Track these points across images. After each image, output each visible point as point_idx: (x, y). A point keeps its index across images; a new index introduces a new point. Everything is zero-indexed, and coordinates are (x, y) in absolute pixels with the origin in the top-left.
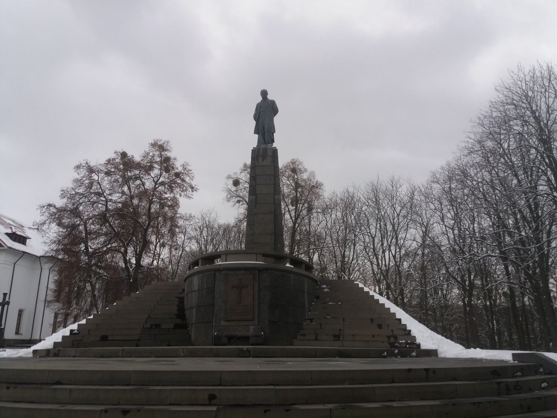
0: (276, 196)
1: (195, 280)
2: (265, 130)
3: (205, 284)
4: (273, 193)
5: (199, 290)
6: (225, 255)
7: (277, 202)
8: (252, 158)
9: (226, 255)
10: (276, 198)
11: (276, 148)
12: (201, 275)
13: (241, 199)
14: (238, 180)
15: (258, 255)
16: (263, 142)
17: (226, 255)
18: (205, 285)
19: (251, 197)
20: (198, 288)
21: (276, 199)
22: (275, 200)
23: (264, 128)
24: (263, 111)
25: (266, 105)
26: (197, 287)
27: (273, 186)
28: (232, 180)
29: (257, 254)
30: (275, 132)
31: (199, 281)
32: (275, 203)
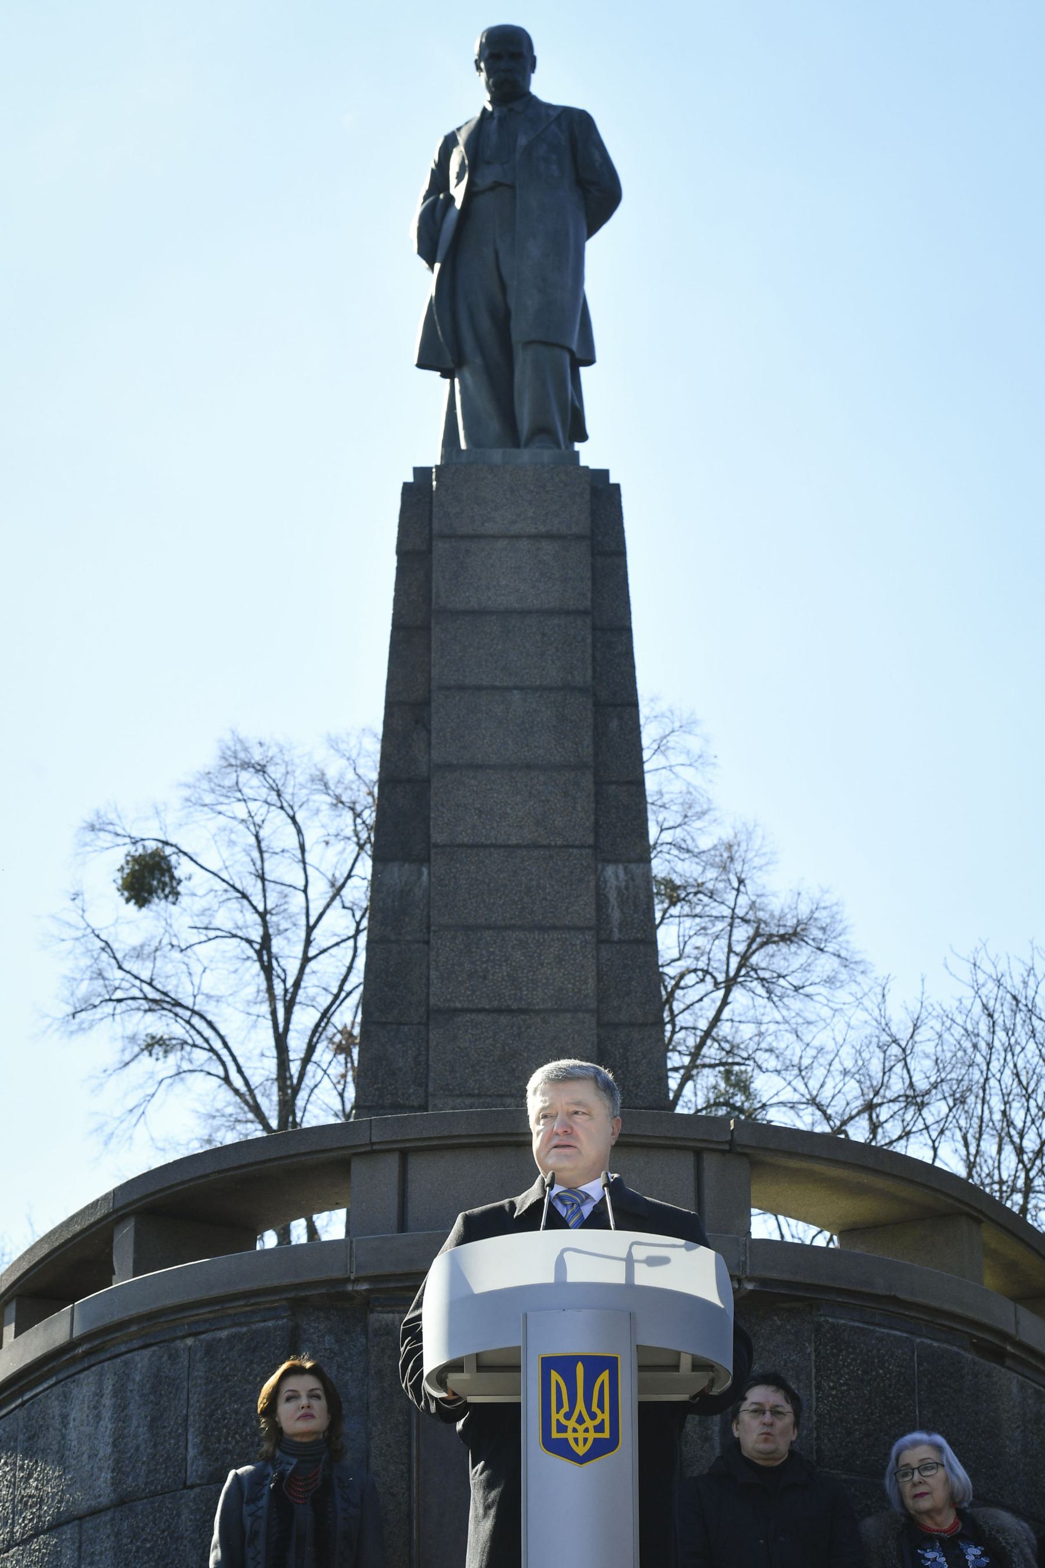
0: (610, 870)
1: (79, 1412)
3: (193, 1438)
4: (590, 840)
5: (122, 1502)
6: (392, 1162)
7: (616, 915)
8: (399, 552)
9: (404, 1154)
10: (612, 882)
11: (605, 473)
12: (142, 1360)
13: (178, 1030)
14: (165, 858)
15: (711, 1163)
16: (494, 426)
17: (404, 1154)
18: (192, 1452)
19: (398, 873)
20: (116, 1483)
21: (613, 896)
22: (601, 903)
23: (502, 321)
24: (492, 189)
25: (522, 141)
26: (106, 1476)
27: (587, 781)
28: (124, 850)
29: (698, 1153)
30: (590, 361)
31: (121, 1408)
32: (600, 928)
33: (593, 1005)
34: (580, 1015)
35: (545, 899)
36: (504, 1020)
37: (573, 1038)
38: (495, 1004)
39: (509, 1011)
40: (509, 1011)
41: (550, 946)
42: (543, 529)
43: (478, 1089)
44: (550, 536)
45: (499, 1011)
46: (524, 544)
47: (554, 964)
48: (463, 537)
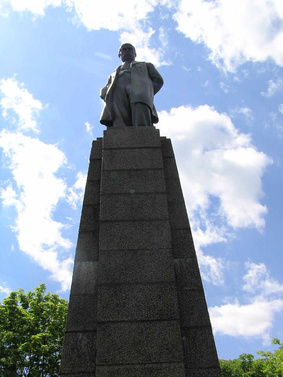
2: (132, 101)
8: (91, 160)
33: (178, 317)
34: (172, 322)
35: (152, 271)
36: (134, 326)
37: (169, 333)
38: (130, 318)
39: (136, 321)
40: (136, 321)
41: (155, 291)
42: (143, 146)
43: (122, 361)
44: (146, 148)
45: (131, 322)
46: (137, 150)
47: (157, 299)
48: (114, 149)
